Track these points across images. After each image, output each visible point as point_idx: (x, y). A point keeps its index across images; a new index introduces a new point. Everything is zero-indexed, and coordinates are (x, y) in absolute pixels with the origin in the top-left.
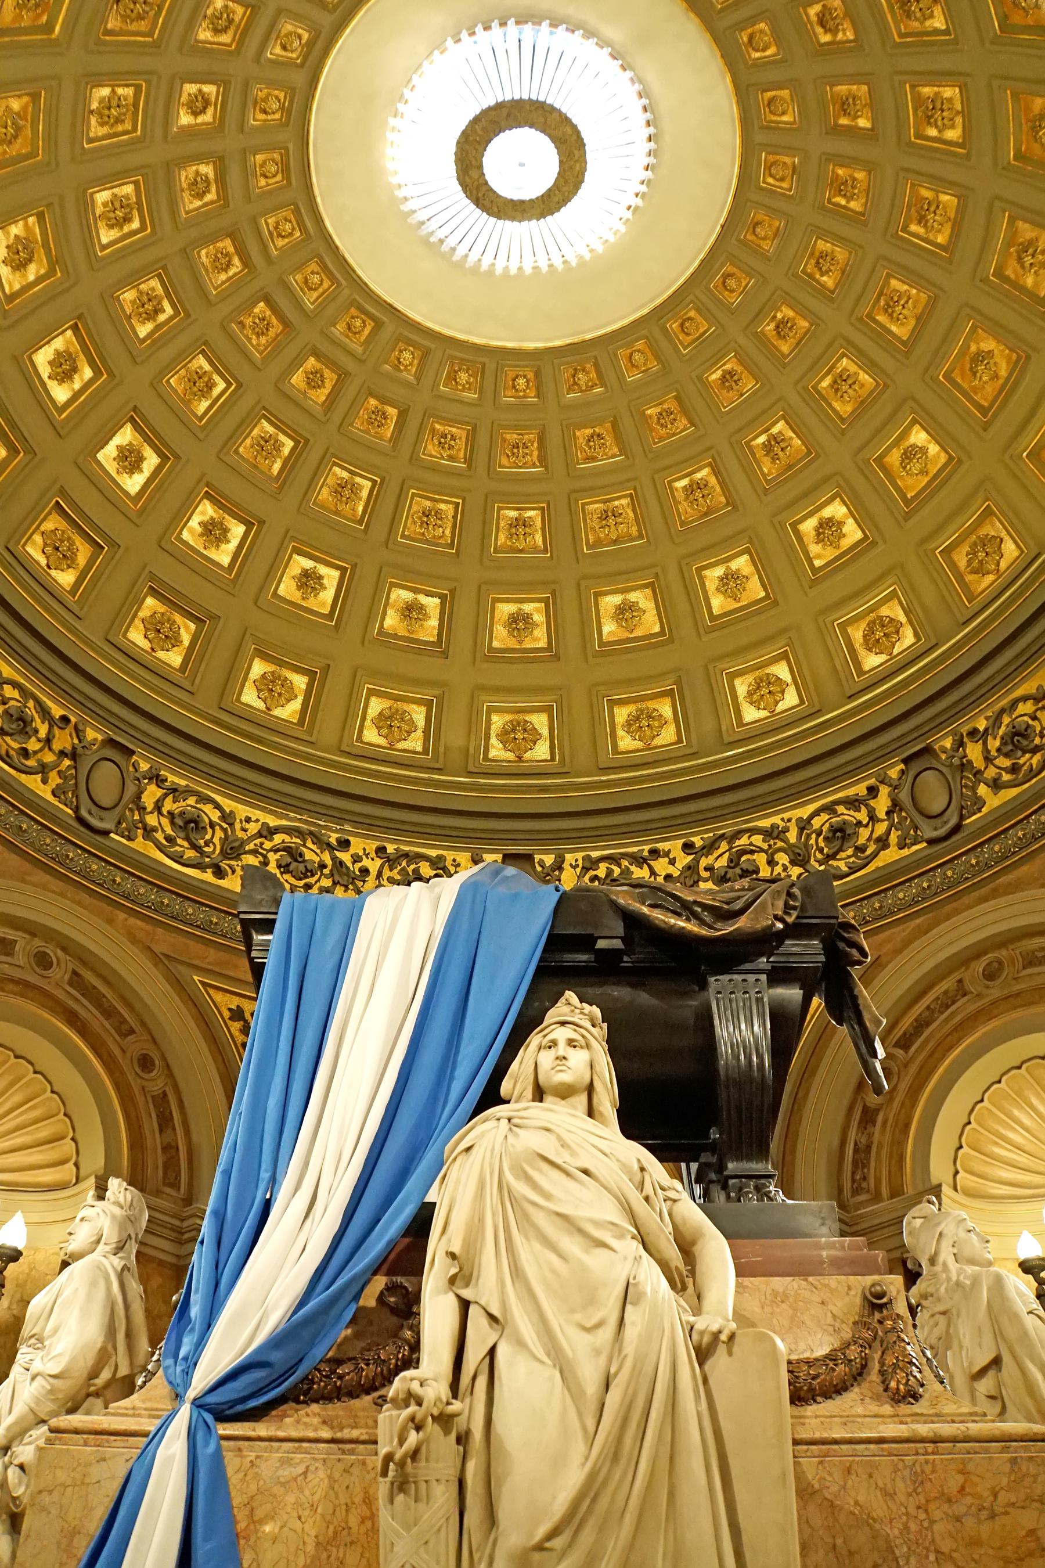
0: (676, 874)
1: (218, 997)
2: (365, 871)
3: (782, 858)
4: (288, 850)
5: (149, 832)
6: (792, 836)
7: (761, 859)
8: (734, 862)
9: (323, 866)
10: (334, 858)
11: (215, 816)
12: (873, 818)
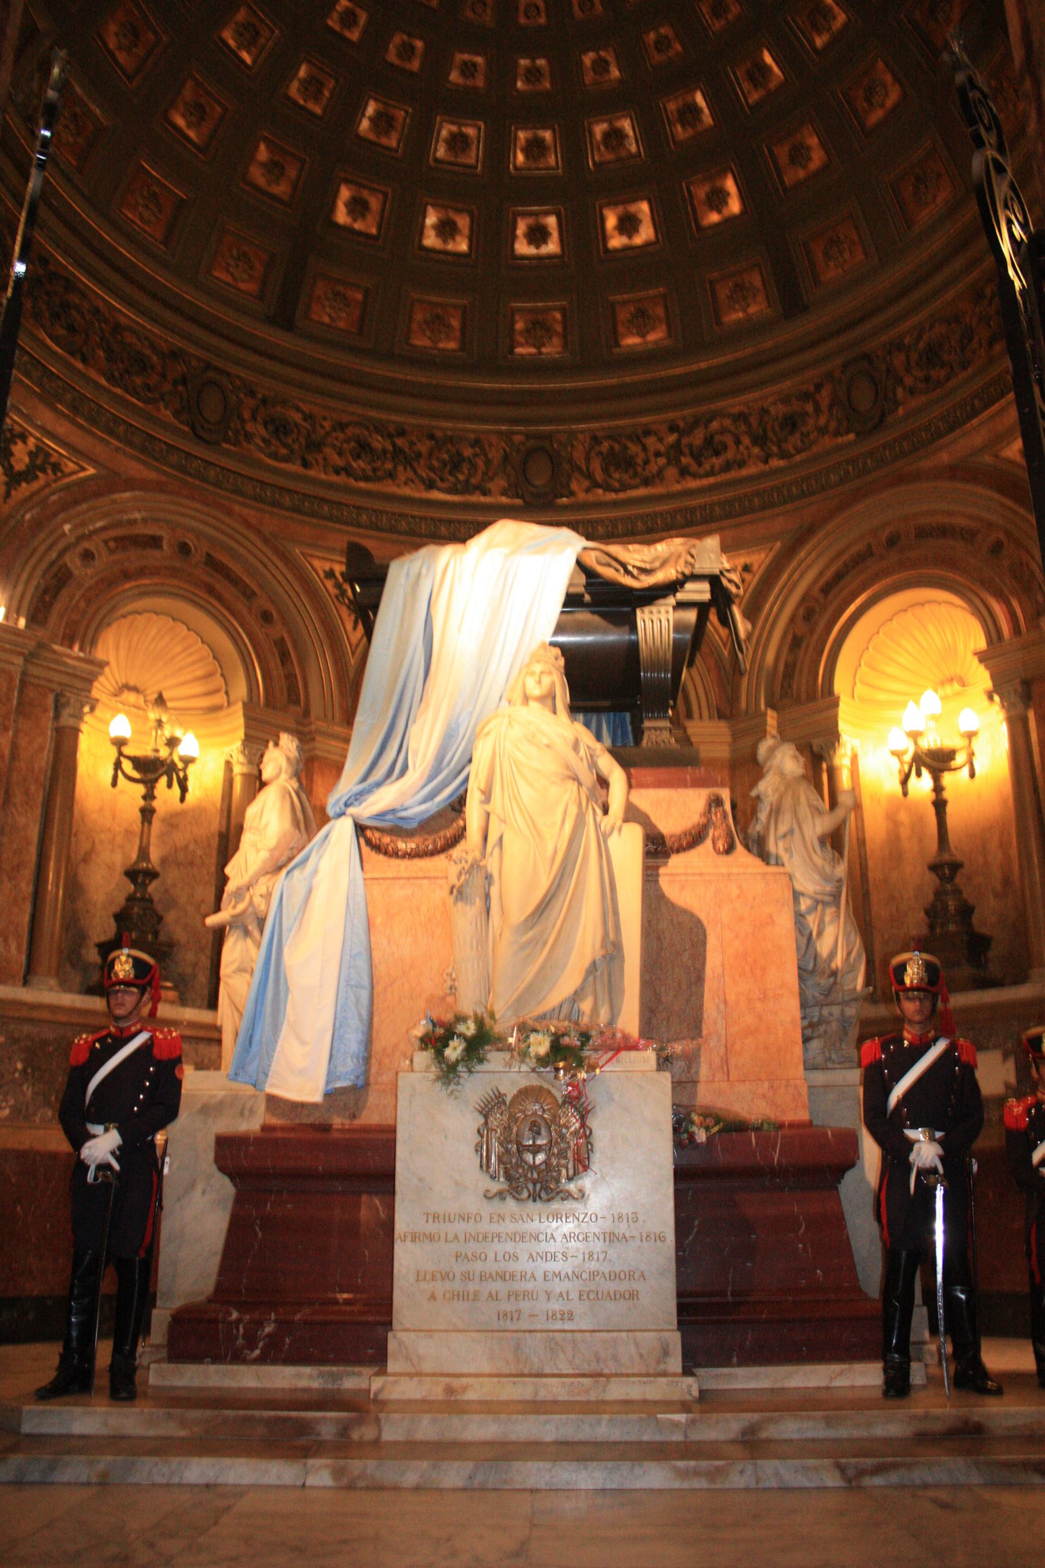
0: (662, 449)
1: (316, 563)
2: (419, 455)
3: (746, 441)
4: (358, 441)
5: (249, 437)
6: (754, 421)
7: (729, 440)
8: (709, 440)
9: (385, 451)
10: (394, 445)
11: (297, 417)
12: (817, 410)
